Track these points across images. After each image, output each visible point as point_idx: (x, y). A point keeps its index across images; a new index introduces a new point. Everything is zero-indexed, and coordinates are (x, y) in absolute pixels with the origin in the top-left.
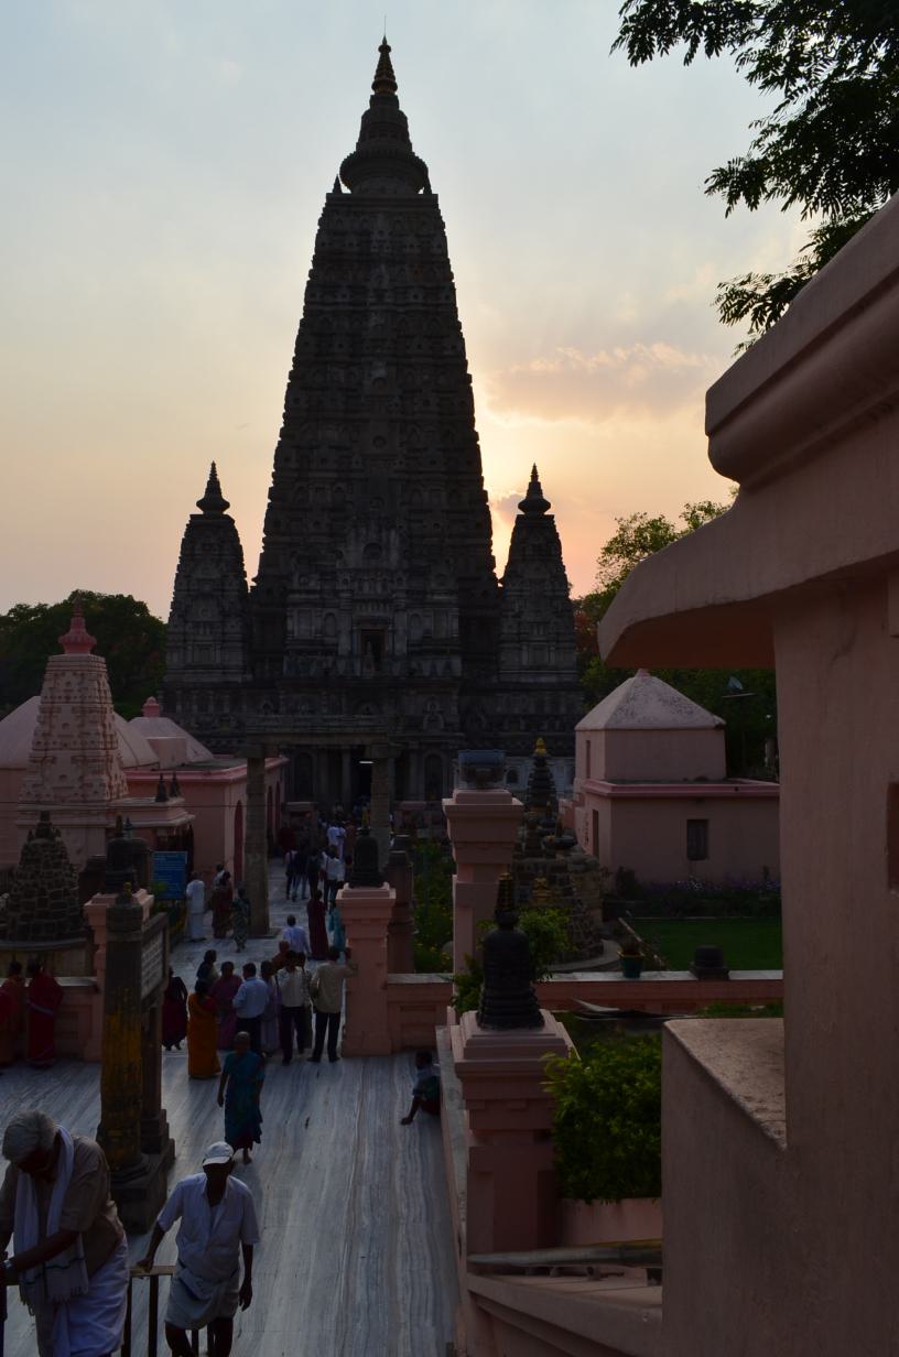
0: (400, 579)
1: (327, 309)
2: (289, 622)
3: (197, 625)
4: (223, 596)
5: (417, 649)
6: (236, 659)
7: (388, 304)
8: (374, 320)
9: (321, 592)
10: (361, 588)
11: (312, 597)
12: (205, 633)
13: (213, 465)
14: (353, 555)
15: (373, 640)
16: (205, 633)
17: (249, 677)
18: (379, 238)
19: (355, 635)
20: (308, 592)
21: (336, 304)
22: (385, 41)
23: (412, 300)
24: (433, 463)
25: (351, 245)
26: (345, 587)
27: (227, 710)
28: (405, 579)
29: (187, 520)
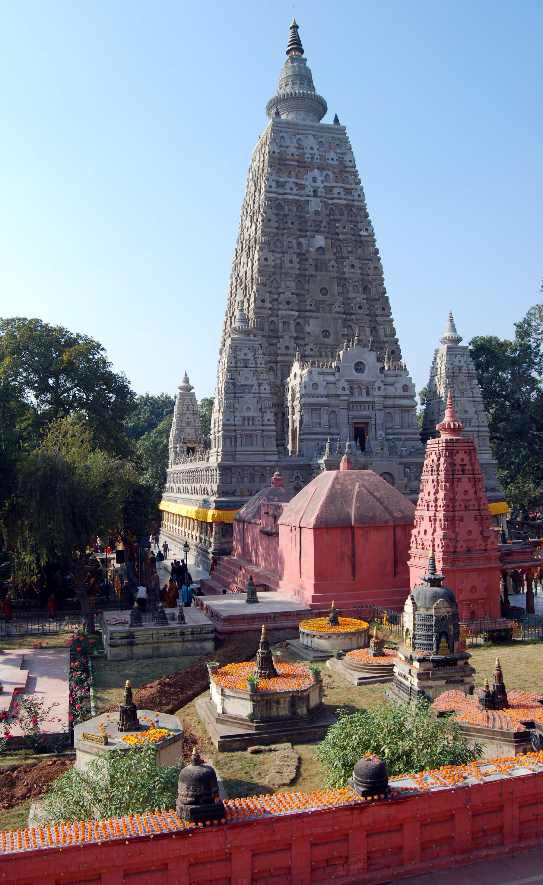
0: (379, 388)
1: (280, 197)
3: (244, 418)
4: (260, 398)
7: (320, 197)
9: (327, 396)
12: (249, 424)
16: (249, 424)
20: (318, 396)
21: (285, 194)
22: (295, 23)
23: (336, 195)
24: (360, 308)
25: (293, 154)
26: (344, 393)
28: (383, 387)
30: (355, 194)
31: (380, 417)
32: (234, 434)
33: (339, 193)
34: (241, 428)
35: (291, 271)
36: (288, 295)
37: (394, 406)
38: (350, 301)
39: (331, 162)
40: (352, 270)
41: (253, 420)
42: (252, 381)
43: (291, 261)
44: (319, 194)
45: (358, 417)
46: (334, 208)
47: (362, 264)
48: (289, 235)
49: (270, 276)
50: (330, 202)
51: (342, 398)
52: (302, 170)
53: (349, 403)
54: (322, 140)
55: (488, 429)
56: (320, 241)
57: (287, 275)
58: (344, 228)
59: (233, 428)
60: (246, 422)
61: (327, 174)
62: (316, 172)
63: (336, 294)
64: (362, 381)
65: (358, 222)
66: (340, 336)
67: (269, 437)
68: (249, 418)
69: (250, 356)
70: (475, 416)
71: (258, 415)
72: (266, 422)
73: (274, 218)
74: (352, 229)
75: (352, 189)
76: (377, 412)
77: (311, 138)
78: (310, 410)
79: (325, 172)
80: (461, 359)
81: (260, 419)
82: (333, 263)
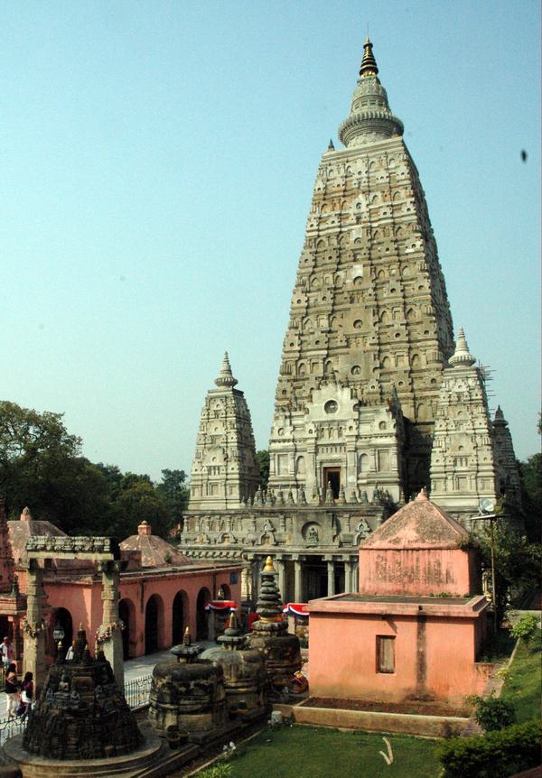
1: (321, 233)
2: (272, 463)
3: (210, 468)
5: (365, 481)
6: (236, 493)
7: (364, 222)
8: (354, 235)
10: (323, 436)
11: (287, 444)
13: (226, 353)
14: (317, 410)
15: (332, 478)
17: (243, 504)
18: (358, 176)
19: (318, 471)
20: (284, 441)
24: (398, 335)
26: (310, 436)
27: (227, 530)
28: (355, 427)
29: (206, 394)
30: (404, 209)
31: (351, 460)
32: (200, 483)
33: (385, 213)
34: (206, 477)
35: (323, 308)
36: (318, 335)
37: (370, 446)
38: (387, 330)
39: (380, 181)
40: (393, 295)
41: (219, 469)
42: (221, 431)
43: (324, 298)
44: (363, 220)
45: (327, 461)
46: (380, 230)
47: (405, 286)
48: (325, 271)
49: (303, 318)
50: (375, 225)
51: (308, 441)
52: (347, 199)
53: (317, 446)
54: (374, 160)
55: (492, 468)
56: (358, 270)
57: (318, 314)
58: (388, 249)
59: (200, 477)
60: (213, 472)
61: (376, 196)
62: (361, 198)
63: (372, 324)
64: (333, 421)
65: (405, 240)
66: (371, 370)
67: (232, 486)
68: (214, 467)
69: (222, 407)
70: (474, 452)
71: (219, 464)
72: (230, 471)
73: (311, 258)
74: (396, 249)
75: (402, 204)
76: (348, 454)
77: (359, 161)
78: (276, 457)
79: (372, 195)
80: (462, 384)
81: (224, 468)
82: (371, 291)
